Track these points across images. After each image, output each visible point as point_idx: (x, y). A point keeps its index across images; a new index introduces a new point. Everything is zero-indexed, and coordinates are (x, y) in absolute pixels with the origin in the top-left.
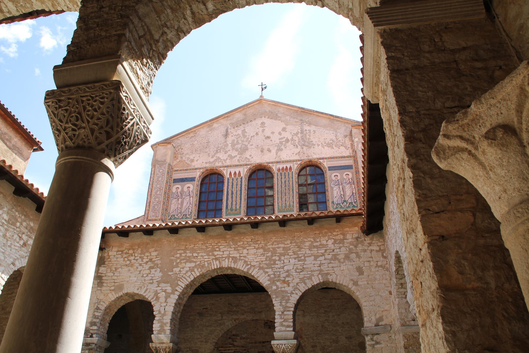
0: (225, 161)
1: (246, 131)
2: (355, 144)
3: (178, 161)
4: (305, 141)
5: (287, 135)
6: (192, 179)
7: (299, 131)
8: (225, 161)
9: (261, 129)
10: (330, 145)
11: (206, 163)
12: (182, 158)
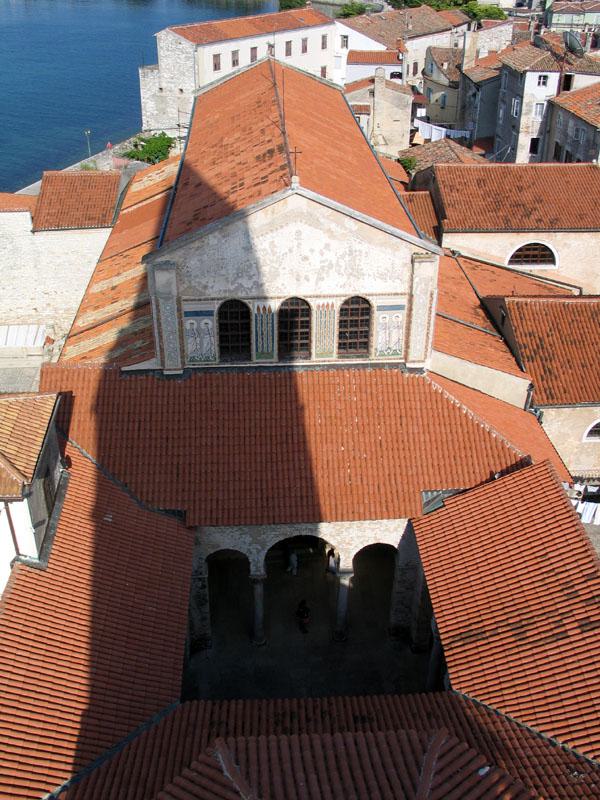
0: (250, 289)
1: (276, 243)
2: (415, 286)
3: (186, 286)
4: (352, 269)
5: (330, 256)
6: (209, 314)
7: (347, 250)
8: (250, 289)
9: (296, 243)
10: (383, 276)
11: (225, 291)
12: (190, 282)
